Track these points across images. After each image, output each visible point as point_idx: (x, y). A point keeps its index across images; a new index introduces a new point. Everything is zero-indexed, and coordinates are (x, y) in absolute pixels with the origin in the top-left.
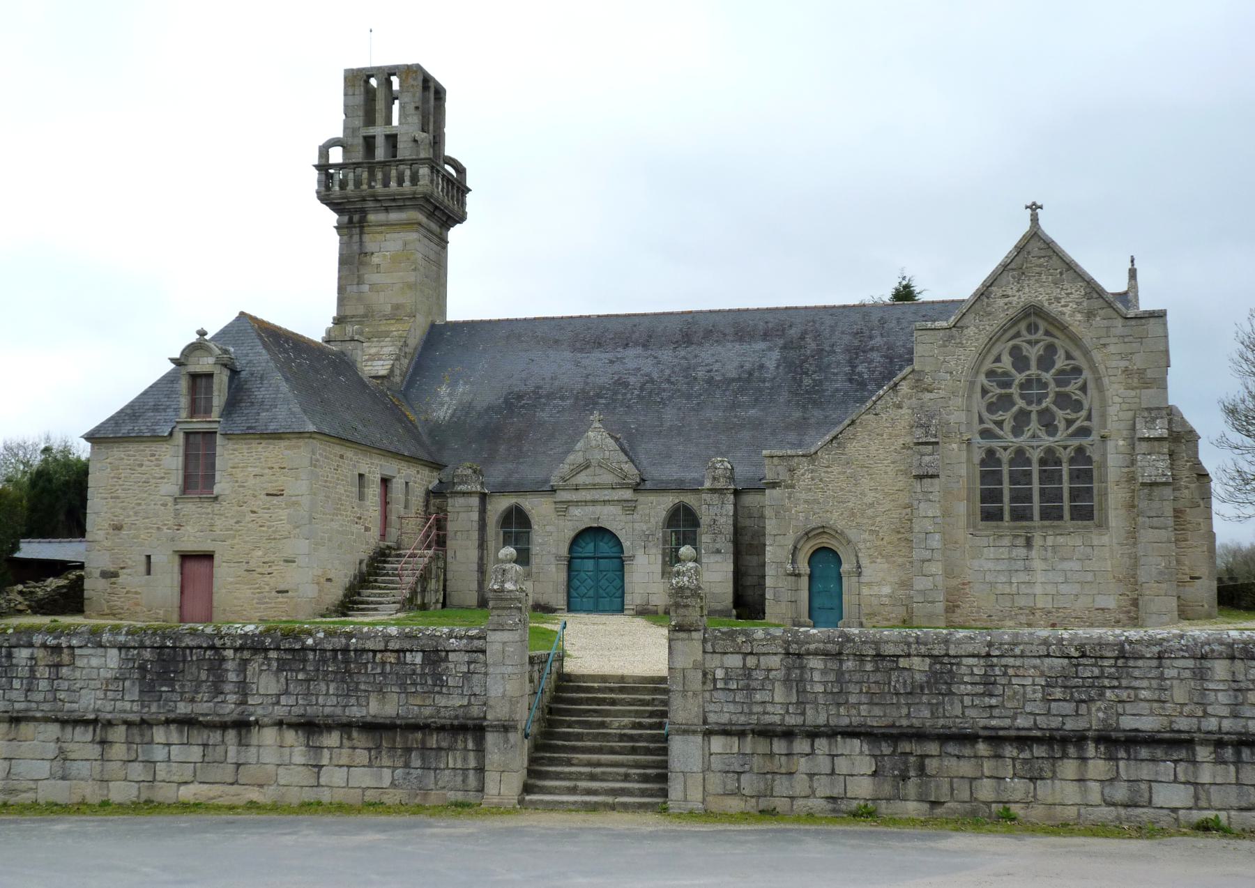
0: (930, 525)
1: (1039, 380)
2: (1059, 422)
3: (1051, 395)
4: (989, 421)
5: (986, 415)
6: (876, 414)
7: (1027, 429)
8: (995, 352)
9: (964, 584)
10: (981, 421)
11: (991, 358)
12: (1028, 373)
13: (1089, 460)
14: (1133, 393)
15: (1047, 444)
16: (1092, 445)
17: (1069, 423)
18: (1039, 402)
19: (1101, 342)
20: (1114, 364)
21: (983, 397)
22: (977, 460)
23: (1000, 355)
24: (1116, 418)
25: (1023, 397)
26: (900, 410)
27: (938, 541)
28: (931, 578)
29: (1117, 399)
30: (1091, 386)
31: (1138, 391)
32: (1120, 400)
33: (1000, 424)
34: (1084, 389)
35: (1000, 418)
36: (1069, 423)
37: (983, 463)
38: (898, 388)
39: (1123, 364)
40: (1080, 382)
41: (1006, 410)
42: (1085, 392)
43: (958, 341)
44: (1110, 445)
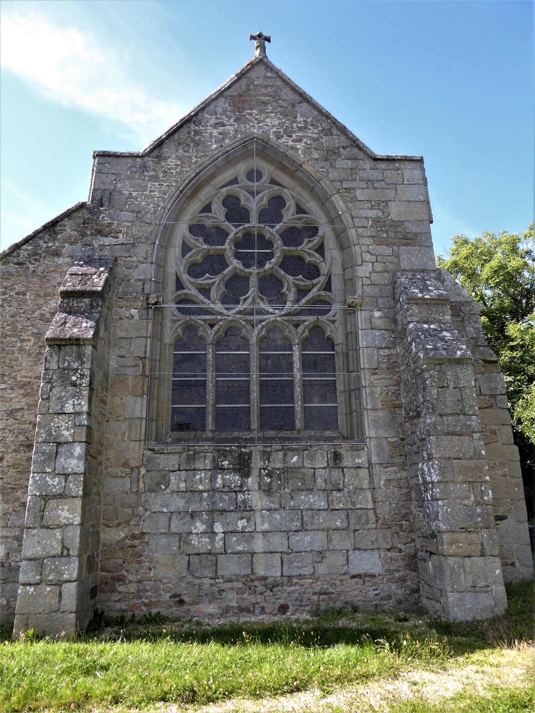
0: (67, 429)
1: (261, 236)
2: (288, 289)
3: (278, 254)
4: (190, 286)
5: (185, 277)
6: (20, 264)
7: (243, 298)
8: (203, 196)
9: (134, 537)
10: (179, 285)
11: (196, 206)
12: (246, 225)
13: (330, 344)
14: (388, 251)
15: (272, 318)
16: (334, 322)
17: (302, 292)
18: (261, 264)
19: (345, 186)
20: (363, 213)
21: (183, 255)
22: (169, 338)
23: (210, 204)
24: (367, 281)
25: (238, 256)
26: (56, 259)
27: (79, 458)
28: (58, 534)
29: (367, 257)
30: (331, 245)
31: (395, 248)
32: (374, 259)
33: (205, 291)
34: (320, 249)
35: (206, 281)
36: (302, 292)
37: (179, 344)
38: (58, 228)
39: (373, 213)
40: (316, 240)
41: (215, 273)
42: (323, 255)
43: (152, 173)
44: (361, 316)
